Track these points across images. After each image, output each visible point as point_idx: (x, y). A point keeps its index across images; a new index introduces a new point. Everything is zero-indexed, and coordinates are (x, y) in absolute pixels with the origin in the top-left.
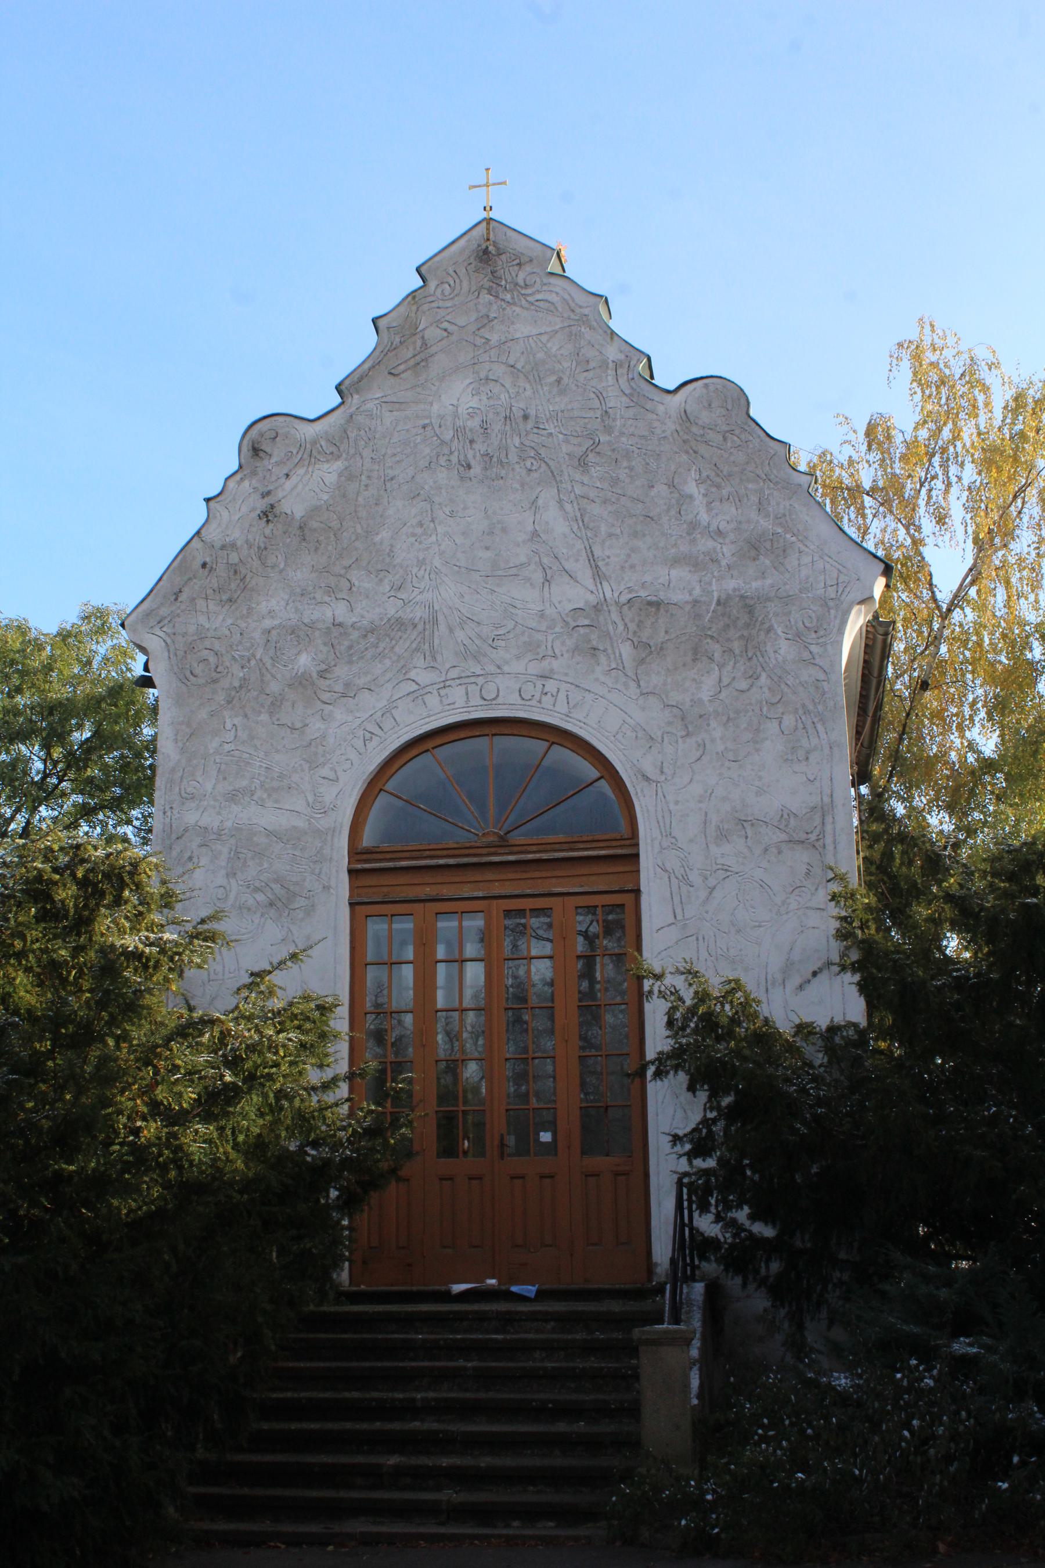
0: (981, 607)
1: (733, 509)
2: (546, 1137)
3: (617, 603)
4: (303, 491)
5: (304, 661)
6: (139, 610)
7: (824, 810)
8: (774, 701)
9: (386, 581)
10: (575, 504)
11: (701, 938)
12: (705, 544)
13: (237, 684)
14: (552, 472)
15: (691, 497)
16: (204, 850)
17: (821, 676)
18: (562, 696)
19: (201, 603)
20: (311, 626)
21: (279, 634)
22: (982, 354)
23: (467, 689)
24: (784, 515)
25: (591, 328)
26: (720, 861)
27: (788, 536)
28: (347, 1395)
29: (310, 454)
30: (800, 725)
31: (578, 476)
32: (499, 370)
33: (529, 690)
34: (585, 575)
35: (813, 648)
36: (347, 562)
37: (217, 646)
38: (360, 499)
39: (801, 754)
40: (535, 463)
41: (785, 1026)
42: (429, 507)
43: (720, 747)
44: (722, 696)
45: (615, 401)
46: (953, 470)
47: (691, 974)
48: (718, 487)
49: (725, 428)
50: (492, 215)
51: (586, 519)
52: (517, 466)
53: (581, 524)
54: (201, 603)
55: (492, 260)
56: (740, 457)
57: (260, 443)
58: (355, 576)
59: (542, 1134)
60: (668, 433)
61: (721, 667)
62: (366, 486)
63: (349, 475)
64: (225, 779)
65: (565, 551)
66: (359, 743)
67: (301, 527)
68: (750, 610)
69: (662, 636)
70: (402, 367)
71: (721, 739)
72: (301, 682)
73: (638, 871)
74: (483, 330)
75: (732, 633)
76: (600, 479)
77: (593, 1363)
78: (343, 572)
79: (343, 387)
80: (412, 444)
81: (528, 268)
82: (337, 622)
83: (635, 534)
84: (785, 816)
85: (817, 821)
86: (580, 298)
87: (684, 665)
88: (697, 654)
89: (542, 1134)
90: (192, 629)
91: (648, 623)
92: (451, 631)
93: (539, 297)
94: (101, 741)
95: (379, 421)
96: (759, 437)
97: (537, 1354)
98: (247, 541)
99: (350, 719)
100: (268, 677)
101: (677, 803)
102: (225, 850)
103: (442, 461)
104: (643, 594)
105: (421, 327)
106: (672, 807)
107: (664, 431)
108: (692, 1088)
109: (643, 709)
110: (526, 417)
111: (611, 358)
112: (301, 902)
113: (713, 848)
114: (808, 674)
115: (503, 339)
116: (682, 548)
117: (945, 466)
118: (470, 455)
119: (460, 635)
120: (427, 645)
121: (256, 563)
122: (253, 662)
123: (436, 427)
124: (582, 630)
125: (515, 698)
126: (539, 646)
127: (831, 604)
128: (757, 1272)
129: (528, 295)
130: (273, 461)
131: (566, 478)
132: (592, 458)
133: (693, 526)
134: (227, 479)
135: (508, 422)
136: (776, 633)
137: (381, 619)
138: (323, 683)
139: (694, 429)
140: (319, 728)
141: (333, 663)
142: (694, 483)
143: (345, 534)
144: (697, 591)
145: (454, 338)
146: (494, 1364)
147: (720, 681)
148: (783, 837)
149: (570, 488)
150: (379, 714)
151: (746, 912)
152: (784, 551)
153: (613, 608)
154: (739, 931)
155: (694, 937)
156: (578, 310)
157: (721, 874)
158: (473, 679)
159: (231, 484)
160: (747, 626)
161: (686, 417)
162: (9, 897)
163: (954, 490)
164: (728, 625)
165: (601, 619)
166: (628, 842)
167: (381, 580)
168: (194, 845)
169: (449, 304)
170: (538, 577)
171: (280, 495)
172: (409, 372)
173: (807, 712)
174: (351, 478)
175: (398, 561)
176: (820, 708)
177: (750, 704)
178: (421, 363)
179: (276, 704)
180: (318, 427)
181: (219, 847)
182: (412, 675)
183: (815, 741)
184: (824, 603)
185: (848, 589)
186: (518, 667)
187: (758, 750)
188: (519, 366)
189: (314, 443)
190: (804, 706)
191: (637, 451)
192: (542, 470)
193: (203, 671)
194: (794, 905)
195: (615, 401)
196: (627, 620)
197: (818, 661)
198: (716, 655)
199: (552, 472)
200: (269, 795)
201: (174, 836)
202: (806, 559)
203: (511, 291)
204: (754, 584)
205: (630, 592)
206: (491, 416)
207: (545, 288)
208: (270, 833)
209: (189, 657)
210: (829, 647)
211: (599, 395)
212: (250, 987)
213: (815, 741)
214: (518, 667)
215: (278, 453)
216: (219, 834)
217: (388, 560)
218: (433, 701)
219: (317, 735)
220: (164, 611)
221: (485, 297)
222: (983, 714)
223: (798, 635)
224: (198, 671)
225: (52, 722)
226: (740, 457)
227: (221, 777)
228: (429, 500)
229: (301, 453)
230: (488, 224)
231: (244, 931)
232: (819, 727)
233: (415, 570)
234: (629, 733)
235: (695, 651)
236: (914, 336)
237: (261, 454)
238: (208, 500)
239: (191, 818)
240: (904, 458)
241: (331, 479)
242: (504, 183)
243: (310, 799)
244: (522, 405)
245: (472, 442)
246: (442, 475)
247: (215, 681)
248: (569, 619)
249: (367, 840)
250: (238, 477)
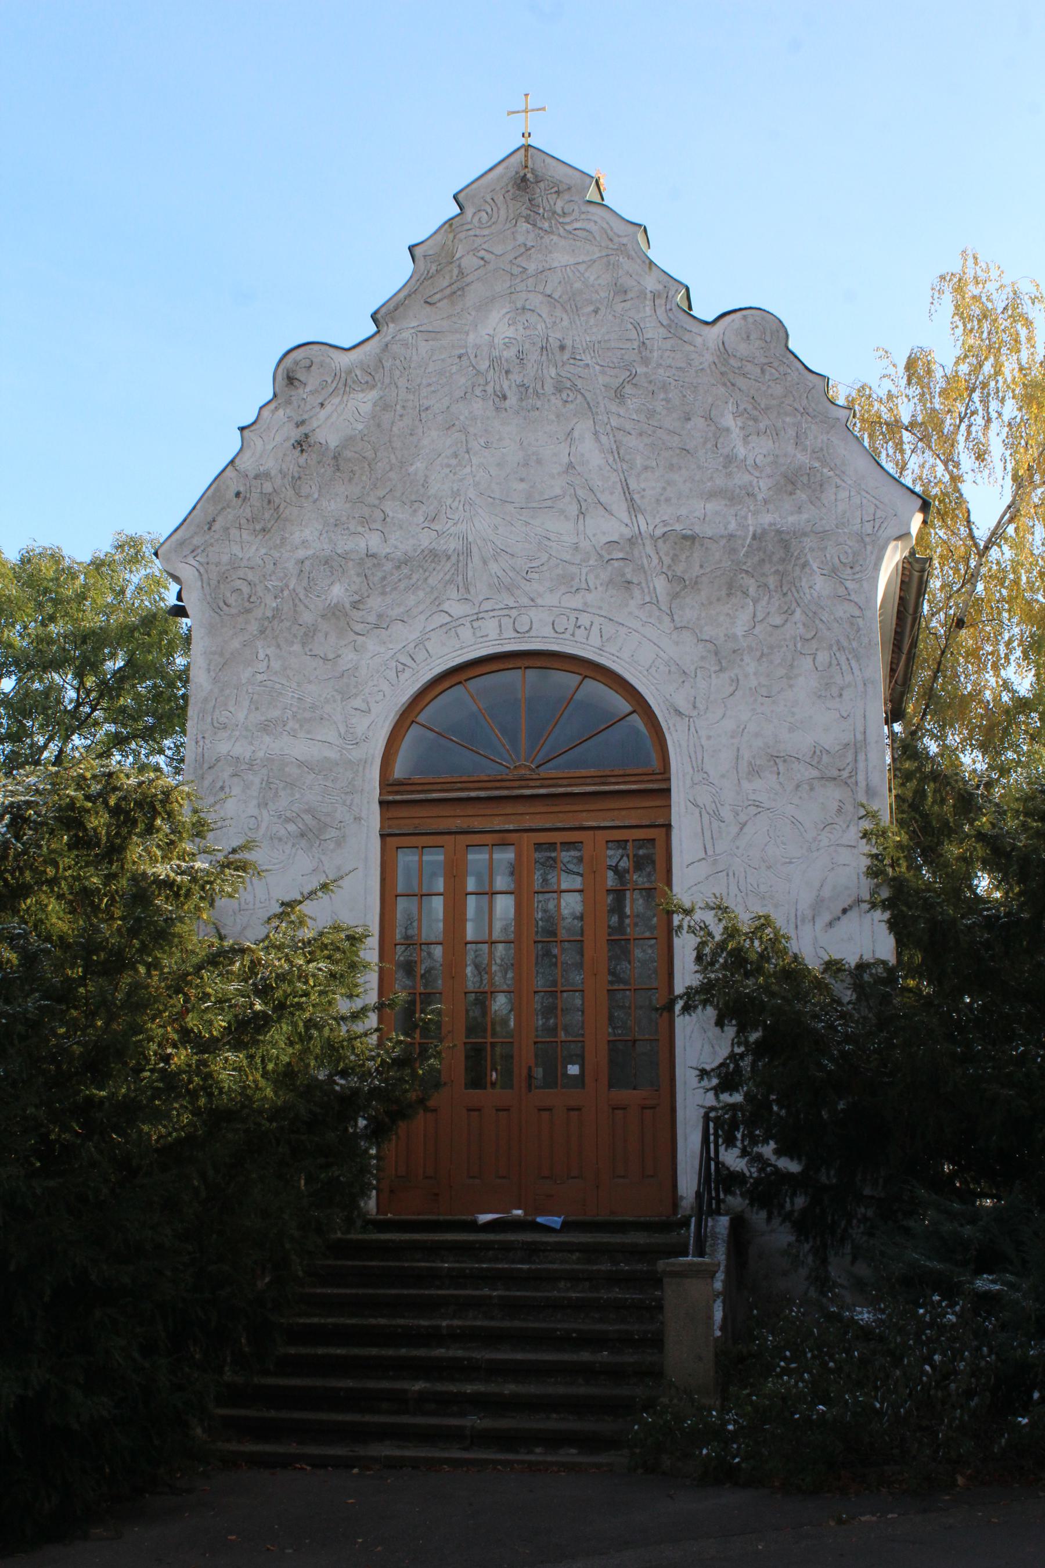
0: (1018, 545)
1: (771, 442)
2: (573, 1070)
3: (652, 536)
4: (336, 421)
5: (338, 592)
6: (173, 538)
7: (857, 747)
8: (809, 636)
9: (420, 512)
10: (611, 436)
11: (731, 874)
12: (742, 478)
13: (269, 614)
14: (588, 404)
15: (728, 430)
16: (236, 779)
17: (857, 613)
18: (595, 630)
19: (234, 532)
20: (345, 557)
21: (312, 564)
22: (1026, 288)
23: (500, 621)
24: (822, 449)
25: (629, 257)
26: (752, 797)
27: (825, 470)
28: (373, 1321)
29: (346, 383)
30: (834, 662)
31: (613, 408)
32: (536, 300)
33: (562, 623)
34: (620, 509)
35: (848, 584)
36: (381, 493)
37: (250, 577)
38: (394, 429)
39: (835, 691)
40: (571, 394)
41: (813, 963)
42: (464, 438)
43: (754, 683)
44: (756, 631)
45: (653, 332)
46: (994, 405)
47: (721, 909)
48: (756, 420)
49: (764, 360)
50: (531, 141)
51: (622, 452)
52: (553, 398)
53: (616, 456)
54: (234, 532)
55: (530, 188)
56: (778, 390)
57: (294, 372)
58: (389, 506)
59: (569, 1066)
60: (705, 365)
61: (755, 602)
62: (401, 416)
63: (384, 405)
64: (257, 709)
65: (600, 483)
66: (392, 674)
67: (335, 457)
68: (786, 545)
69: (696, 571)
70: (438, 296)
71: (755, 674)
72: (335, 613)
73: (670, 806)
74: (519, 259)
75: (767, 568)
76: (638, 411)
77: (616, 1293)
78: (377, 502)
79: (379, 316)
80: (448, 374)
81: (566, 196)
82: (370, 552)
83: (671, 467)
84: (818, 753)
85: (850, 758)
86: (619, 228)
87: (718, 600)
88: (732, 588)
89: (569, 1066)
90: (225, 558)
91: (683, 557)
92: (485, 563)
93: (578, 225)
94: (133, 670)
95: (414, 349)
96: (797, 369)
97: (562, 1285)
98: (281, 471)
99: (382, 650)
100: (301, 608)
101: (709, 738)
102: (257, 781)
103: (478, 392)
104: (678, 527)
105: (458, 256)
106: (704, 741)
107: (701, 364)
108: (720, 1023)
109: (677, 643)
110: (562, 348)
111: (649, 289)
112: (332, 833)
113: (745, 784)
114: (842, 610)
115: (541, 269)
116: (717, 482)
117: (985, 401)
119: (494, 567)
120: (460, 577)
121: (290, 493)
122: (286, 593)
123: (472, 357)
124: (616, 564)
125: (548, 631)
126: (573, 579)
127: (867, 539)
128: (782, 1206)
129: (568, 223)
130: (308, 389)
131: (603, 409)
132: (628, 389)
133: (730, 459)
134: (261, 408)
135: (545, 352)
136: (811, 569)
137: (415, 550)
138: (356, 615)
139: (732, 361)
140: (352, 660)
141: (366, 594)
142: (731, 416)
143: (379, 464)
144: (733, 526)
145: (490, 267)
146: (518, 1294)
147: (754, 616)
148: (815, 773)
149: (606, 420)
150: (412, 645)
151: (777, 848)
152: (821, 486)
153: (648, 542)
154: (769, 868)
155: (724, 873)
156: (616, 239)
157: (753, 810)
158: (506, 612)
159: (266, 413)
160: (783, 560)
161: (724, 351)
162: (42, 824)
163: (994, 426)
164: (763, 560)
165: (636, 553)
166: (659, 777)
167: (415, 511)
168: (226, 775)
169: (486, 232)
170: (573, 509)
171: (315, 424)
172: (445, 301)
173: (841, 648)
174: (386, 407)
175: (432, 492)
176: (855, 644)
177: (785, 640)
178: (456, 293)
179: (309, 634)
181: (251, 777)
182: (446, 606)
183: (848, 678)
184: (861, 538)
185: (884, 525)
186: (550, 600)
187: (791, 686)
188: (556, 296)
189: (349, 372)
190: (838, 642)
191: (674, 383)
192: (578, 401)
193: (236, 601)
194: (825, 842)
195: (653, 332)
196: (661, 554)
197: (853, 597)
198: (751, 589)
199: (588, 404)
200: (301, 726)
201: (206, 766)
202: (843, 495)
203: (549, 219)
204: (791, 519)
205: (665, 526)
206: (527, 346)
207: (583, 216)
208: (301, 764)
209: (222, 586)
210: (865, 584)
211: (637, 326)
212: (280, 916)
213: (848, 678)
214: (550, 600)
215: (312, 381)
216: (251, 765)
217: (422, 490)
218: (466, 633)
219: (349, 666)
220: (197, 541)
221: (523, 226)
222: (1018, 653)
223: (834, 570)
224: (231, 600)
225: (85, 651)
226: (778, 390)
227: (253, 707)
228: (464, 430)
229: (335, 383)
230: (526, 151)
231: (276, 861)
232: (853, 663)
233: (449, 501)
234: (662, 667)
235: (730, 586)
236: (957, 269)
237: (296, 383)
238: (242, 429)
239: (223, 748)
240: (944, 393)
241: (366, 408)
242: (543, 109)
243: (342, 731)
244: (559, 336)
245: (507, 372)
246: (477, 406)
247: (248, 611)
248: (603, 553)
249: (399, 771)
250: (272, 406)
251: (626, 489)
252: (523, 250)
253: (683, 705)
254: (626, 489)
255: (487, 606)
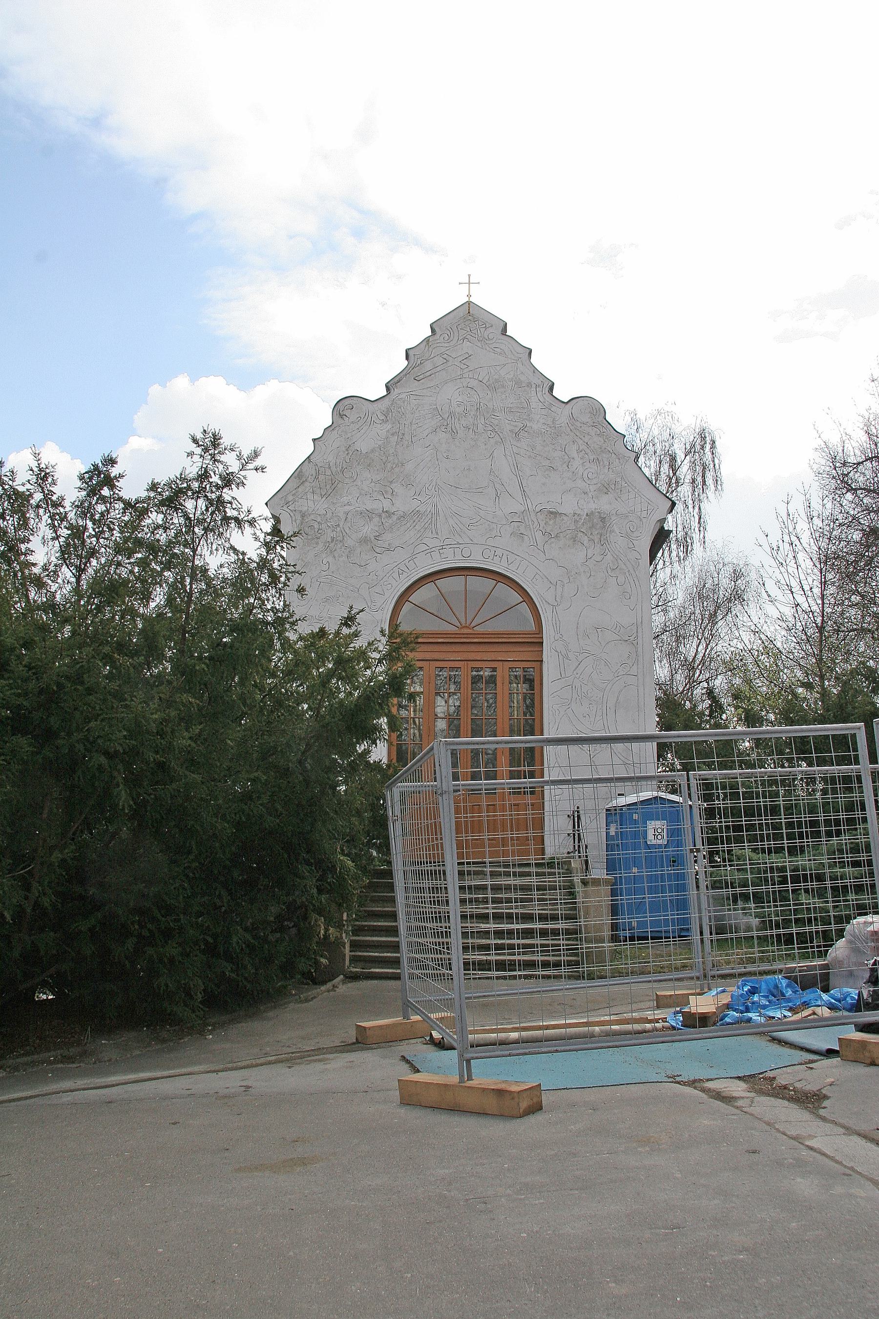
18: (505, 557)
66: (396, 575)
68: (603, 520)
72: (364, 541)
153: (533, 514)
169: (446, 345)
180: (375, 405)
218: (436, 555)
220: (290, 498)
238: (314, 440)
251: (521, 485)
253: (551, 600)
254: (521, 485)
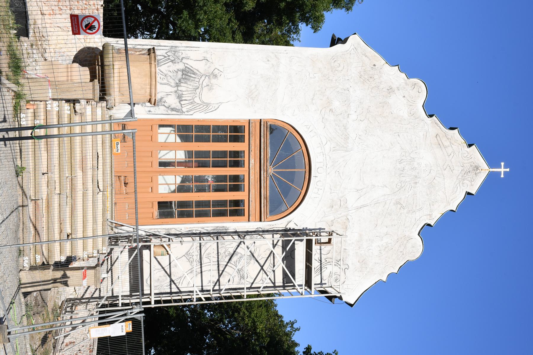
5: (336, 104)
49: (405, 253)
81: (469, 183)
103: (403, 154)
104: (350, 224)
118: (404, 163)
122: (338, 84)
130: (410, 91)
132: (399, 206)
139: (405, 242)
169: (460, 156)
182: (328, 143)
201: (276, 54)
252: (452, 169)
255: (328, 158)
